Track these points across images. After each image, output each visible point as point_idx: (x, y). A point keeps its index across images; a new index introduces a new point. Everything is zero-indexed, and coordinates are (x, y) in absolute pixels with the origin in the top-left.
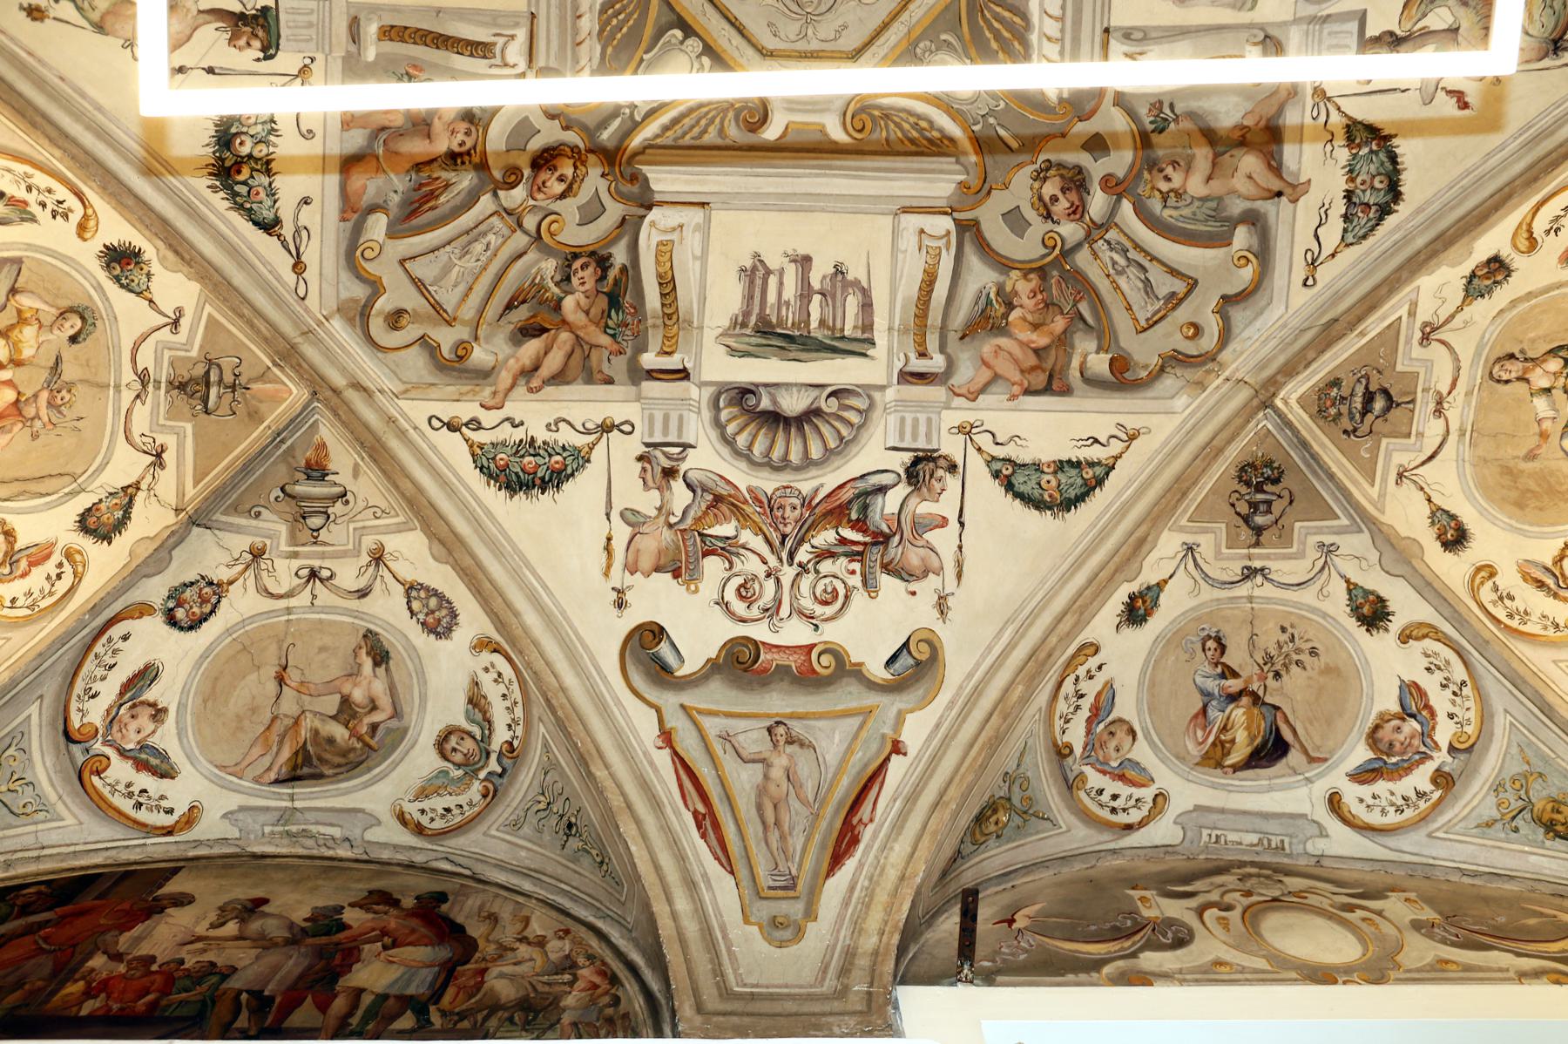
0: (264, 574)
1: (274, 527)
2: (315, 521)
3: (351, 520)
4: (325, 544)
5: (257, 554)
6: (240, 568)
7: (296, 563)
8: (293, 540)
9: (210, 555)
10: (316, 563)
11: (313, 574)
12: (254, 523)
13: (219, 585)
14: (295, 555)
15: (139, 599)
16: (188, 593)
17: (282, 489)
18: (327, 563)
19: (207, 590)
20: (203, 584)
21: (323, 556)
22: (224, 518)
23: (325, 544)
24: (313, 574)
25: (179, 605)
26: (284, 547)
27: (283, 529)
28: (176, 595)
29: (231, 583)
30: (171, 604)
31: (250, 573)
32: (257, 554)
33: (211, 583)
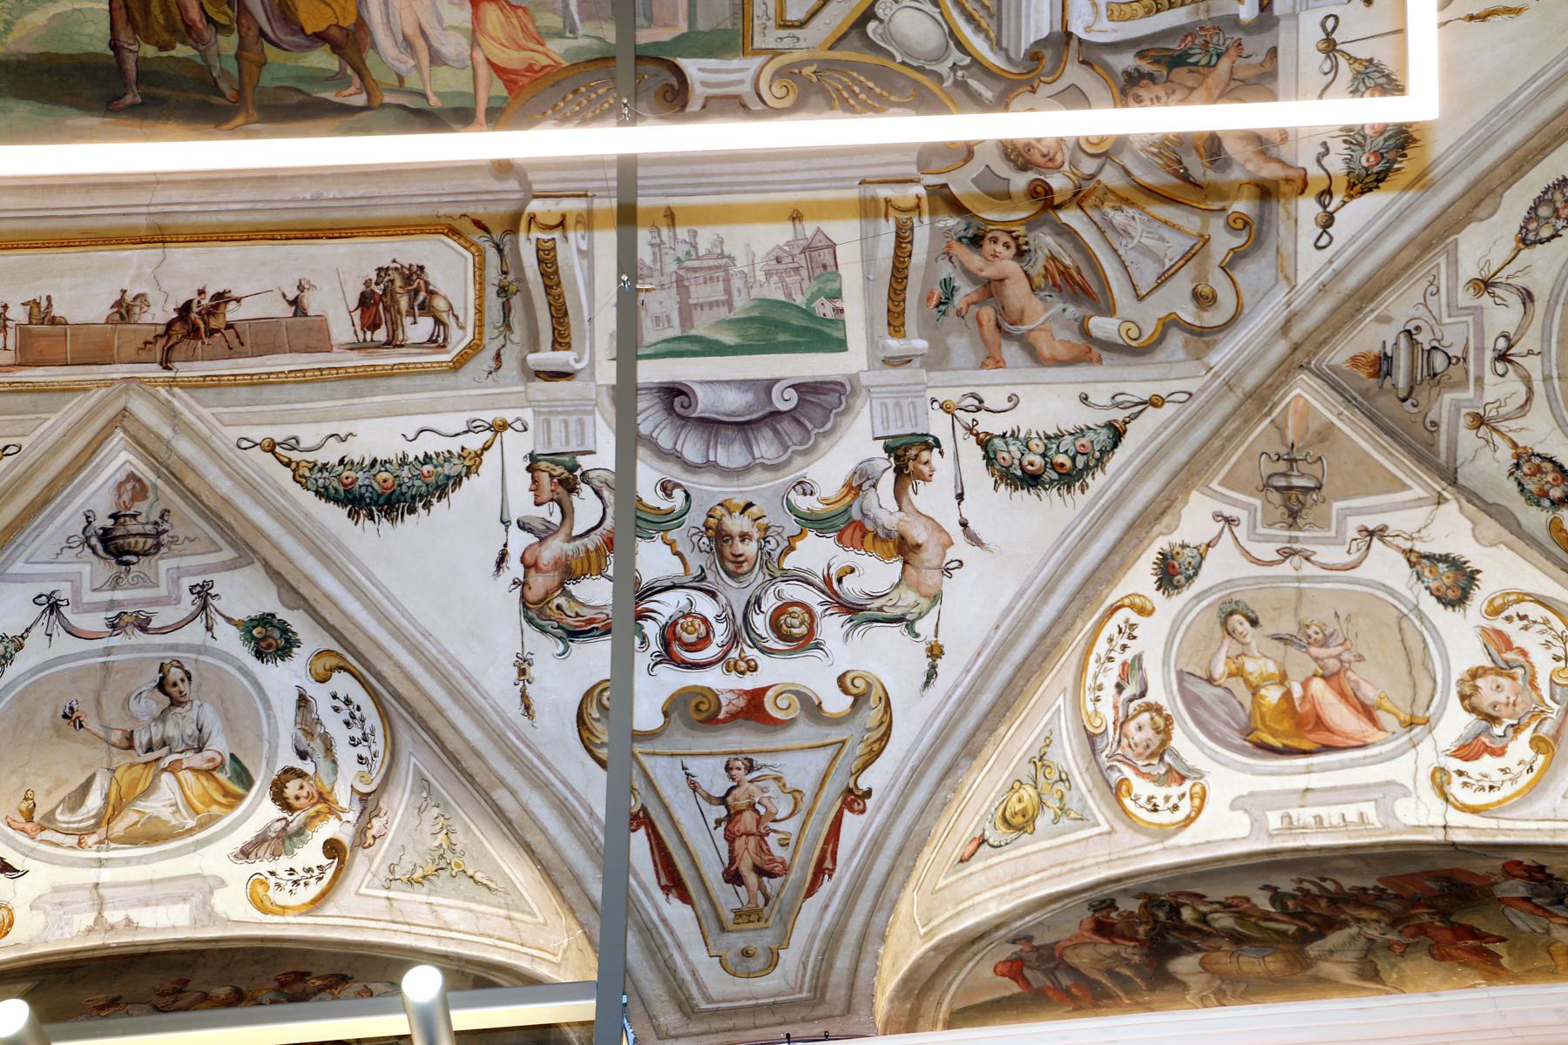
0: (1502, 411)
1: (1447, 405)
2: (1439, 362)
3: (1438, 321)
4: (1466, 349)
5: (1479, 421)
6: (1496, 437)
7: (1489, 378)
8: (1462, 384)
9: (1488, 463)
10: (1489, 355)
11: (1503, 357)
12: (1443, 428)
13: (1519, 457)
14: (1479, 380)
15: (1546, 533)
16: (1532, 486)
17: (1404, 400)
18: (1489, 344)
19: (1526, 469)
20: (1519, 474)
21: (1480, 349)
22: (1443, 457)
23: (1466, 349)
24: (1503, 357)
25: (1546, 495)
26: (1470, 393)
27: (1448, 397)
28: (1535, 499)
29: (1515, 445)
30: (1547, 503)
31: (1502, 426)
32: (1479, 421)
33: (1517, 466)
